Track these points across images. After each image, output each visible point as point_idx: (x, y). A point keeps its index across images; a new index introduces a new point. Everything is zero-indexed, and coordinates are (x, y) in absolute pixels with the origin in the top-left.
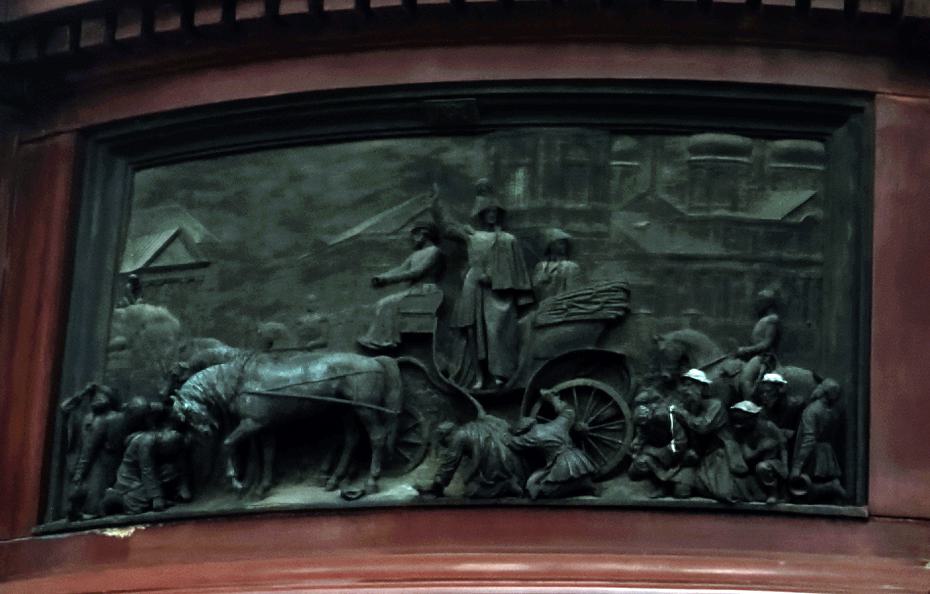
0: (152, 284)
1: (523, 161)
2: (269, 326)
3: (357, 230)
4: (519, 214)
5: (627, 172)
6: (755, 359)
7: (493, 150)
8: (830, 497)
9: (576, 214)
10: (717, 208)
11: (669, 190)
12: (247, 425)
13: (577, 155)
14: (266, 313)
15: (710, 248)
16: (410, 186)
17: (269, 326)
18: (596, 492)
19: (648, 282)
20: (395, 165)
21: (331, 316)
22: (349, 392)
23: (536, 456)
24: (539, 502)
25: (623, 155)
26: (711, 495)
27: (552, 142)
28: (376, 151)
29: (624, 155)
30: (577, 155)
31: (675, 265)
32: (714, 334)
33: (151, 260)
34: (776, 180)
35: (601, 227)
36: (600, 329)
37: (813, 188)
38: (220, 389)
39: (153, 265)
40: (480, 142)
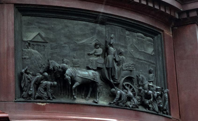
0: (33, 45)
3: (83, 41)
12: (77, 84)
22: (96, 79)
23: (129, 98)
27: (118, 29)
28: (84, 24)
29: (128, 35)
33: (32, 39)
39: (33, 40)
40: (104, 26)
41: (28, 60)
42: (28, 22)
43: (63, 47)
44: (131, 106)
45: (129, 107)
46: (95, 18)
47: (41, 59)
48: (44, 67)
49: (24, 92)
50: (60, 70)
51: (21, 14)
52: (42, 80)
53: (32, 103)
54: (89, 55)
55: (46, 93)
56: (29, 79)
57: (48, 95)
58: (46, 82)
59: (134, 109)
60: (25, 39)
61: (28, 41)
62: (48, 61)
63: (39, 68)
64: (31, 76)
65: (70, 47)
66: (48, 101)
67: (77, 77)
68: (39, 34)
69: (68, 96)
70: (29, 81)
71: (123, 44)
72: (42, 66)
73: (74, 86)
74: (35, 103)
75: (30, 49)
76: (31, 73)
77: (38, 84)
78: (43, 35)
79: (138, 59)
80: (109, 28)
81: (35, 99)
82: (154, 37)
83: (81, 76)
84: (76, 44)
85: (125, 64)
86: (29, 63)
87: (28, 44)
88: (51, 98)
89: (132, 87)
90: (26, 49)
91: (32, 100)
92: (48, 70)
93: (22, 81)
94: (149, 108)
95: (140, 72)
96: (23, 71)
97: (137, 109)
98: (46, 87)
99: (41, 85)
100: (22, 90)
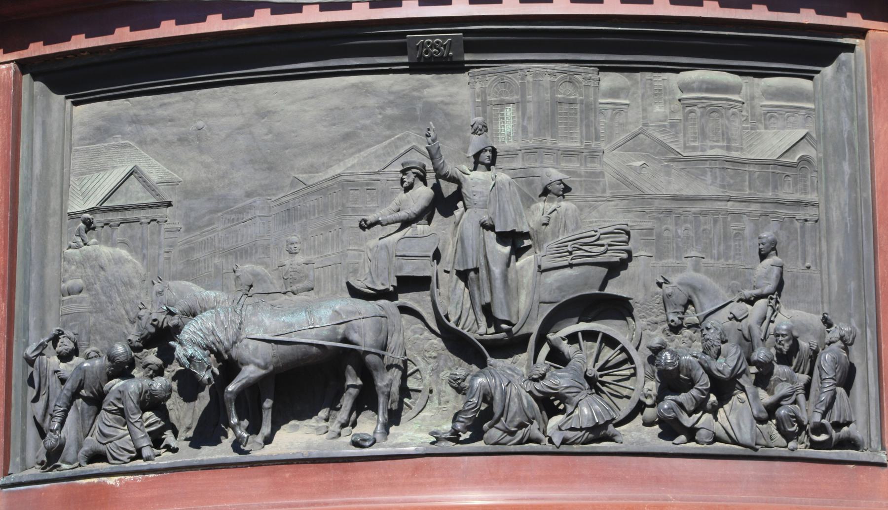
1: (509, 98)
2: (247, 268)
3: (337, 170)
4: (512, 154)
5: (619, 110)
6: (762, 303)
7: (478, 86)
8: (850, 443)
9: (569, 154)
10: (712, 148)
11: (662, 129)
12: (249, 373)
13: (566, 92)
14: (243, 253)
15: (706, 188)
16: (391, 123)
17: (247, 268)
18: (616, 438)
19: (648, 224)
20: (372, 101)
21: (313, 257)
22: (354, 337)
24: (564, 448)
25: (614, 93)
26: (735, 442)
28: (353, 85)
30: (566, 92)
31: (673, 205)
32: (717, 275)
33: (105, 200)
34: (769, 115)
35: (597, 167)
36: (604, 271)
37: (804, 127)
38: (221, 336)
40: (464, 77)
41: (81, 295)
42: (98, 129)
44: (557, 440)
45: (550, 441)
46: (401, 50)
47: (136, 281)
51: (67, 98)
52: (110, 378)
54: (365, 226)
59: (576, 448)
63: (127, 323)
66: (140, 463)
67: (245, 341)
71: (576, 145)
73: (231, 388)
78: (155, 172)
79: (675, 198)
80: (491, 79)
82: (818, 72)
83: (267, 337)
84: (305, 186)
85: (561, 238)
86: (85, 307)
87: (82, 224)
89: (620, 343)
90: (79, 247)
94: (691, 433)
95: (684, 260)
97: (606, 445)
98: (121, 406)
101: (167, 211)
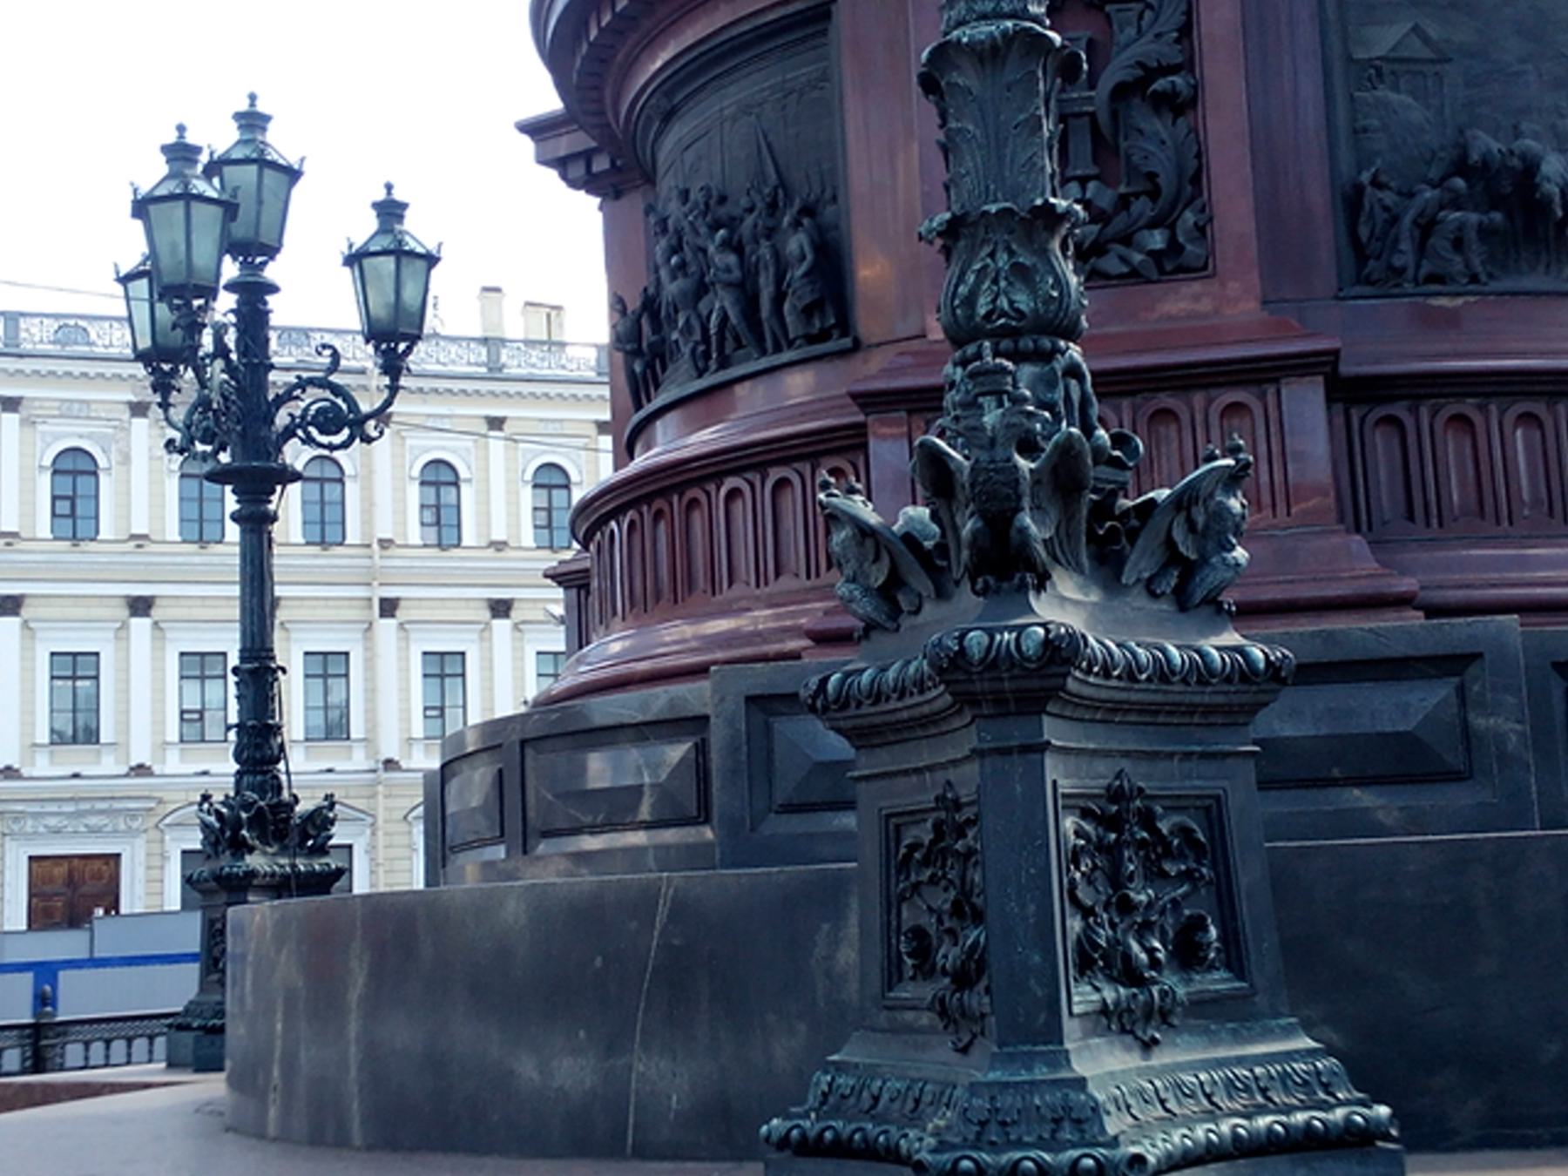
33: (1393, 49)
43: (1518, 74)
47: (1427, 127)
48: (1441, 159)
49: (1372, 263)
50: (1515, 162)
52: (1442, 208)
53: (1406, 300)
55: (1458, 258)
56: (1386, 209)
57: (1467, 265)
58: (1458, 214)
60: (1360, 54)
61: (1371, 60)
62: (1461, 132)
64: (1396, 198)
65: (1540, 76)
66: (1471, 287)
68: (1416, 29)
69: (1548, 266)
70: (1386, 215)
72: (1433, 159)
74: (1420, 299)
75: (1383, 92)
76: (1392, 184)
77: (1426, 227)
78: (1433, 32)
81: (1417, 284)
88: (1483, 278)
90: (1367, 90)
91: (1409, 287)
92: (1461, 166)
93: (1362, 219)
96: (1365, 177)
99: (1438, 227)
100: (1360, 252)
101: (1447, 67)
